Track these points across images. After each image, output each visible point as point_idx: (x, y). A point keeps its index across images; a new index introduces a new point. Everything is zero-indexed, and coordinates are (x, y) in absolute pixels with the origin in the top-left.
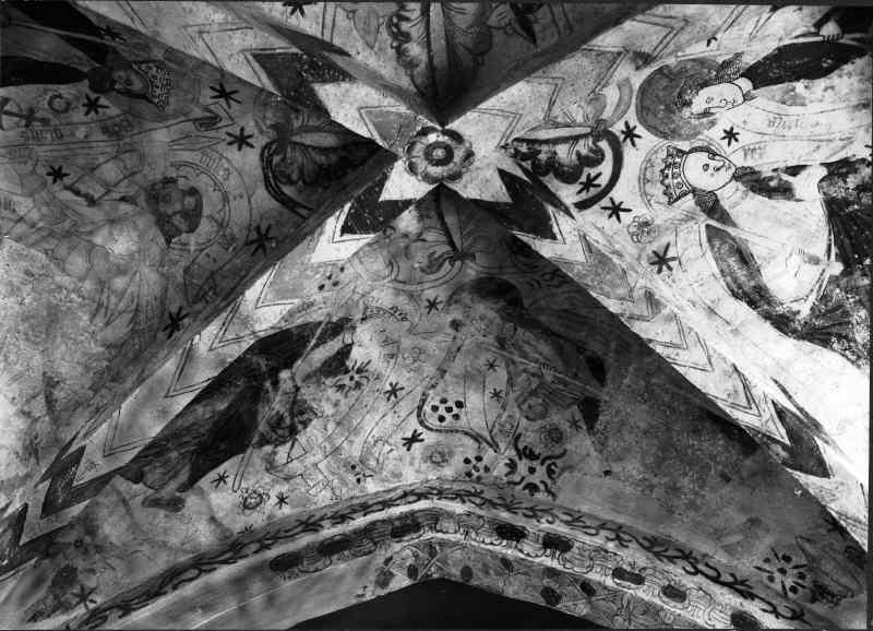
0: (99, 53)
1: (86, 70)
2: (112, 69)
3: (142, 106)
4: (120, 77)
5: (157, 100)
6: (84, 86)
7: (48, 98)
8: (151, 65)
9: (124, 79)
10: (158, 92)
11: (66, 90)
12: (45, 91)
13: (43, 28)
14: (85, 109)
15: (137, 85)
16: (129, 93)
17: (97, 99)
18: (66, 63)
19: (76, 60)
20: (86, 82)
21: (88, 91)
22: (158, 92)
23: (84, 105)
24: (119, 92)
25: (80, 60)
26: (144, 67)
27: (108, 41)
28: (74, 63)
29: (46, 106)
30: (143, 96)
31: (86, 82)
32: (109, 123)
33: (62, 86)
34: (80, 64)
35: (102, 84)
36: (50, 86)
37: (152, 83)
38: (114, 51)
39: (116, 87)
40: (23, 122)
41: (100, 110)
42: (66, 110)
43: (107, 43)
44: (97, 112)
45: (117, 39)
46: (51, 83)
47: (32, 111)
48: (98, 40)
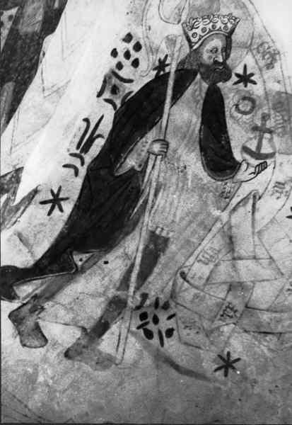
0: (185, 77)
1: (205, 86)
2: (201, 65)
3: (239, 36)
4: (210, 57)
5: (230, 26)
6: (226, 87)
7: (240, 115)
8: (190, 34)
9: (211, 54)
10: (219, 25)
11: (230, 102)
12: (232, 116)
13: (165, 116)
14: (249, 84)
15: (218, 43)
16: (227, 49)
17: (238, 75)
18: (202, 102)
19: (197, 93)
20: (220, 85)
21: (229, 84)
22: (219, 25)
23: (246, 86)
24: (227, 56)
25: (197, 88)
26: (193, 40)
27: (172, 68)
28: (200, 94)
29: (248, 116)
30: (228, 37)
31: (220, 85)
32: (262, 63)
33: (226, 102)
34: (201, 90)
35: (220, 71)
36: (227, 114)
37: (210, 31)
38: (182, 63)
39: (221, 60)
40: (267, 135)
41: (248, 73)
42: (253, 101)
43: (173, 71)
44: (252, 75)
45: (167, 62)
46: (224, 112)
47: (255, 129)
48: (172, 77)
